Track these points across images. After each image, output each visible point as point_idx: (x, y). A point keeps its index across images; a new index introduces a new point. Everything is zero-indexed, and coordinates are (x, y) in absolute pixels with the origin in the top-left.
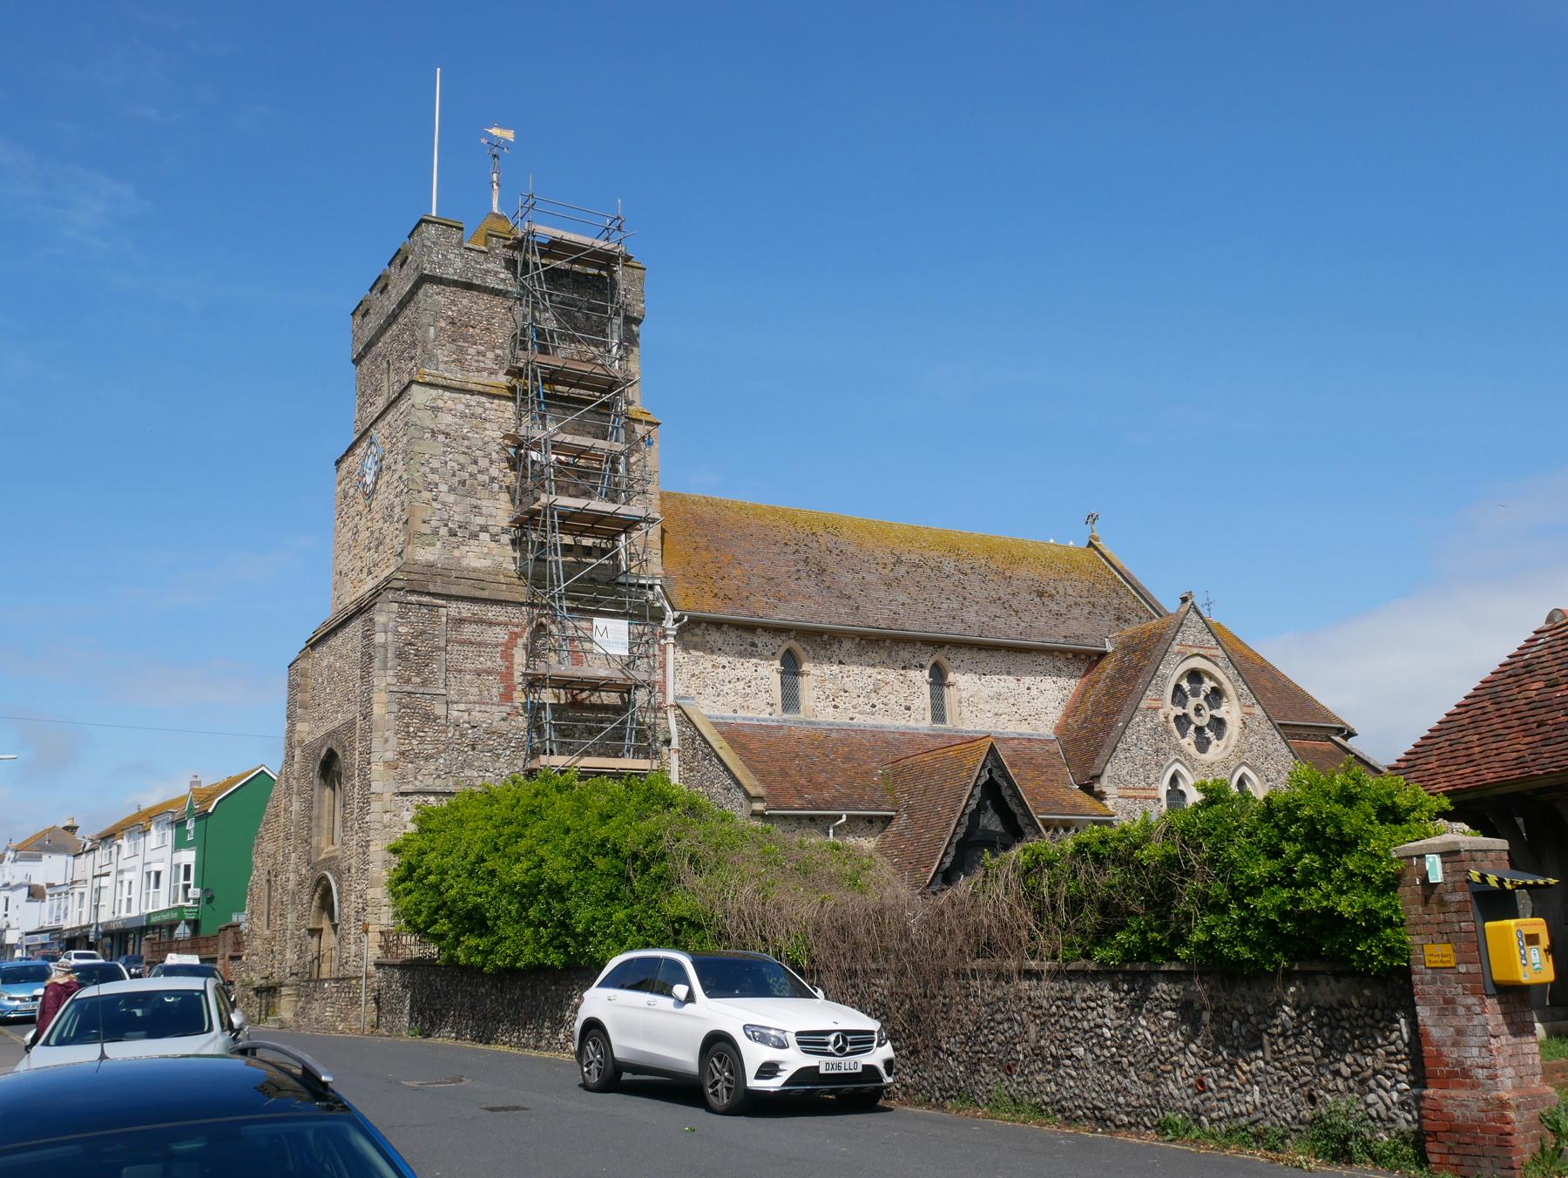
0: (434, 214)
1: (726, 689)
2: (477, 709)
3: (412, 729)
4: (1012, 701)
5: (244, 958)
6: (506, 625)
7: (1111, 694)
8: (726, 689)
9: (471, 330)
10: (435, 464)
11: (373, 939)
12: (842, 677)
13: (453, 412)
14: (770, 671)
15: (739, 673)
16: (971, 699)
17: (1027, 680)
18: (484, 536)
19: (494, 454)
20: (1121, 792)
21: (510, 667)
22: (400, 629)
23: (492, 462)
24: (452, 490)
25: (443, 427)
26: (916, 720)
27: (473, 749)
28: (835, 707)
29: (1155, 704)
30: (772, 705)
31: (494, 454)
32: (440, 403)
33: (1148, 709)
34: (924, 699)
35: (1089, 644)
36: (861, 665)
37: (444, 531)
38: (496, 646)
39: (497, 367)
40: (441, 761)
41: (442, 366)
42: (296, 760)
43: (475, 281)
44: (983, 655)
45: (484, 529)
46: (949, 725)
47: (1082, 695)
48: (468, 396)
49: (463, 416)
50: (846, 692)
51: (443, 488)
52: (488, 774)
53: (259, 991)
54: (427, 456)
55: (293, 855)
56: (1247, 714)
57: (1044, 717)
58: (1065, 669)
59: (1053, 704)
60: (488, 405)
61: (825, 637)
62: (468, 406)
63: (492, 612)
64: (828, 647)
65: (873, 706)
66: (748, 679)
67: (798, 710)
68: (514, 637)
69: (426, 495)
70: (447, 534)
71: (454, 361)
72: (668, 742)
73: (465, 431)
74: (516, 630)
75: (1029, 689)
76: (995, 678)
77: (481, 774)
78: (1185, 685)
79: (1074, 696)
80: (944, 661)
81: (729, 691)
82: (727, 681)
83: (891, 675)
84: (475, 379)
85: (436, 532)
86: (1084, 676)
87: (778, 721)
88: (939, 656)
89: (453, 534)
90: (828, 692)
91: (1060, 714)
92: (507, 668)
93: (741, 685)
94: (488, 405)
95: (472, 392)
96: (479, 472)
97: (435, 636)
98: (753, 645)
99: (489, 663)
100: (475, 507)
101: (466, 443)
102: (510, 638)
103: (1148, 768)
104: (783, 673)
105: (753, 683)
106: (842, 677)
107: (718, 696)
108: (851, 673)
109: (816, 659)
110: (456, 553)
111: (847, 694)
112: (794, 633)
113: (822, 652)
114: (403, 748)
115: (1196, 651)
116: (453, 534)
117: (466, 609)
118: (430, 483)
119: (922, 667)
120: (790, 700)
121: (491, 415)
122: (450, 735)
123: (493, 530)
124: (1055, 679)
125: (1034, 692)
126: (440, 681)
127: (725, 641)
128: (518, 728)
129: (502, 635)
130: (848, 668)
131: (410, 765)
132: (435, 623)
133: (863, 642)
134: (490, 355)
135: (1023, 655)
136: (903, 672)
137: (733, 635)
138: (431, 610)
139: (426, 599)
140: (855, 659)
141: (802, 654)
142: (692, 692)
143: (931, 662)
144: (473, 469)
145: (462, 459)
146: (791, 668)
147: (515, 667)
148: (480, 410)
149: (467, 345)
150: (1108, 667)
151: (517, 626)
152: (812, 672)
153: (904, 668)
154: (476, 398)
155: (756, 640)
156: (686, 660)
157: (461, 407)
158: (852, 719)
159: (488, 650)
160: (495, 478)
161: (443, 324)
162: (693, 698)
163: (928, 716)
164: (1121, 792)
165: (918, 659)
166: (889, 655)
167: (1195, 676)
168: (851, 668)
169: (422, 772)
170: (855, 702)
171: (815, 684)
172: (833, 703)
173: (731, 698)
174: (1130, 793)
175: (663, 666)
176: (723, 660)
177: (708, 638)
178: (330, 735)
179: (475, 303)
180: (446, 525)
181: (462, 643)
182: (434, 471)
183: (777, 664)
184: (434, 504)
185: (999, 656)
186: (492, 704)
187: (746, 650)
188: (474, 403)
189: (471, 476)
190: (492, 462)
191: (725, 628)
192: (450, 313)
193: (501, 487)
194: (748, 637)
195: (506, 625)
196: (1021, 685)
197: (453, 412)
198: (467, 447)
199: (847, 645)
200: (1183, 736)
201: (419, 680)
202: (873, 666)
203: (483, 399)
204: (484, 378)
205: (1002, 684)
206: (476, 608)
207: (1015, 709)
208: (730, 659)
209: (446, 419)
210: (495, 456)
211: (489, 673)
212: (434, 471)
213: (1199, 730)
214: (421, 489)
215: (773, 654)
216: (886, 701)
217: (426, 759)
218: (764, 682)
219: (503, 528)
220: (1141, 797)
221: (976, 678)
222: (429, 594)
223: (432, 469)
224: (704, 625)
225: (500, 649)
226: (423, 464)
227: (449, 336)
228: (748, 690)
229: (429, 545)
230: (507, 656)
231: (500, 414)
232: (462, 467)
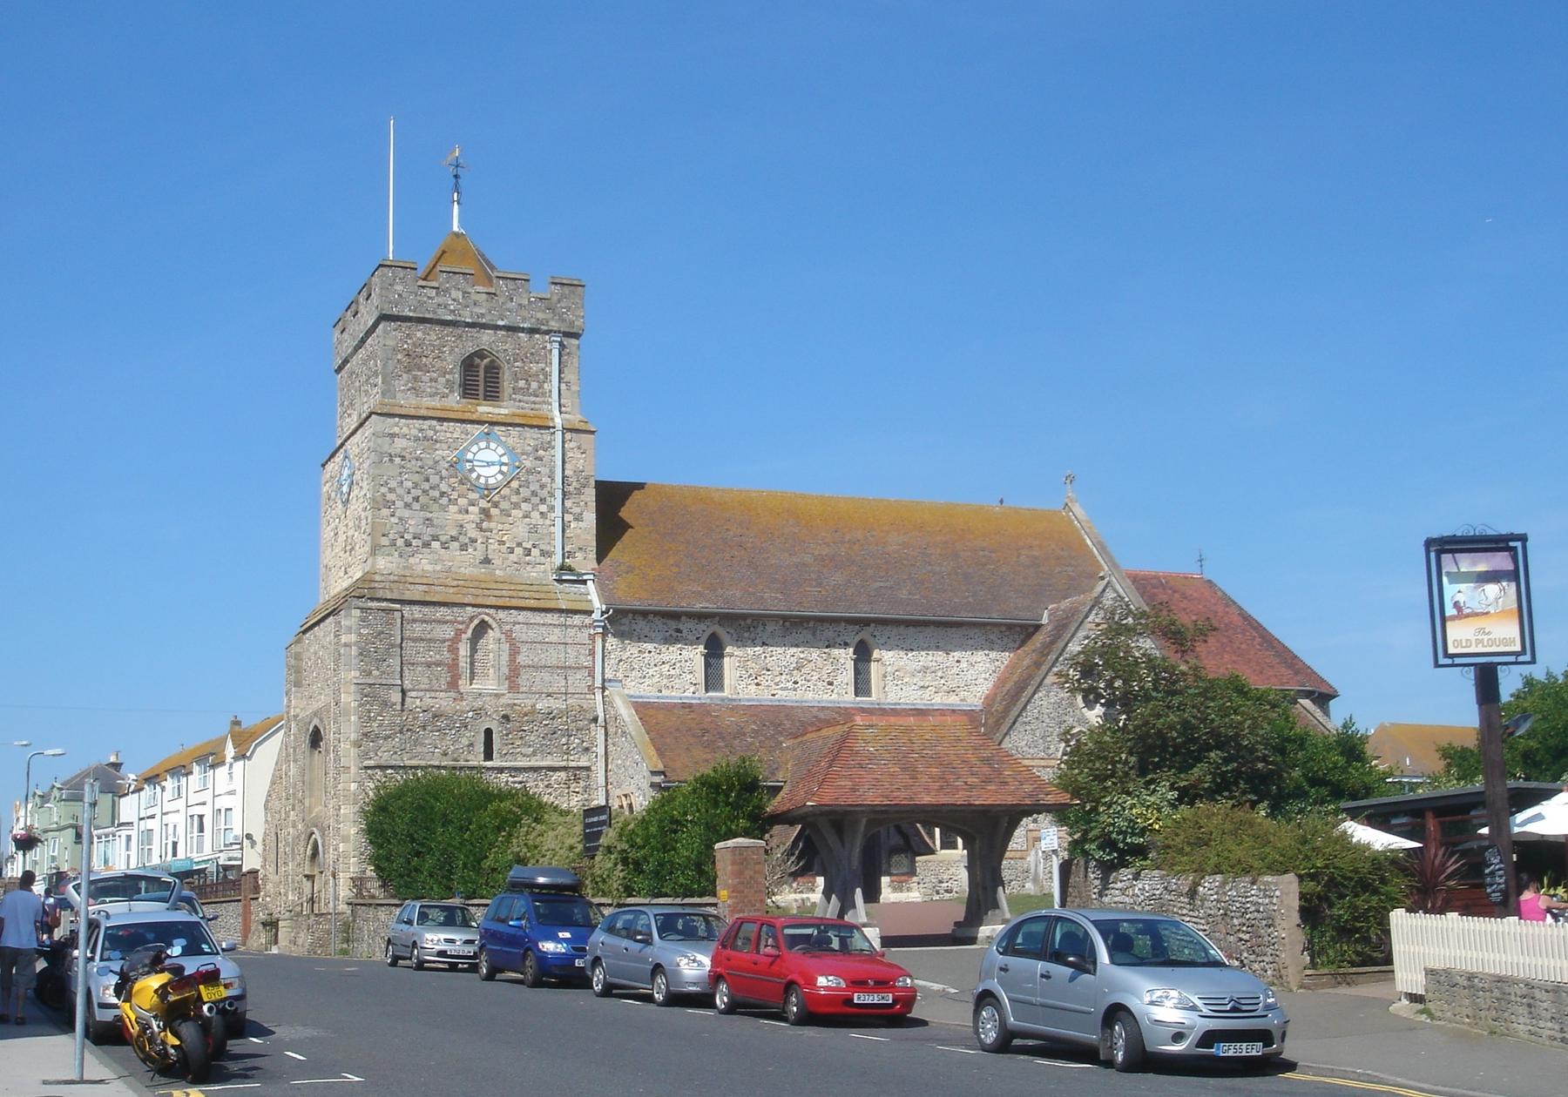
0: (391, 258)
1: (651, 672)
2: (428, 696)
3: (372, 715)
4: (940, 674)
5: (260, 899)
6: (452, 622)
7: (1038, 665)
8: (651, 672)
9: (424, 359)
10: (393, 484)
11: (344, 879)
13: (408, 437)
14: (695, 656)
15: (665, 657)
16: (897, 673)
17: (957, 655)
18: (436, 545)
19: (444, 471)
21: (456, 659)
22: (362, 631)
23: (442, 478)
24: (407, 506)
25: (398, 451)
26: (838, 694)
27: (425, 730)
28: (757, 684)
30: (695, 684)
31: (444, 471)
32: (396, 430)
34: (847, 676)
35: (1024, 616)
36: (785, 645)
37: (400, 542)
38: (444, 641)
39: (447, 391)
40: (397, 740)
41: (399, 395)
42: (292, 732)
43: (427, 316)
44: (911, 629)
45: (435, 538)
46: (874, 698)
47: (1012, 667)
48: (421, 422)
49: (417, 439)
50: (769, 670)
51: (399, 504)
52: (437, 750)
53: (264, 924)
54: (385, 478)
55: (292, 812)
57: (973, 688)
58: (999, 641)
59: (983, 676)
60: (438, 428)
62: (421, 430)
63: (442, 612)
64: (752, 629)
65: (796, 683)
66: (673, 661)
67: (721, 689)
68: (459, 633)
69: (385, 512)
70: (403, 545)
71: (408, 390)
72: (595, 720)
73: (418, 452)
74: (460, 627)
75: (958, 661)
76: (923, 653)
77: (431, 750)
79: (1006, 667)
80: (870, 641)
81: (655, 674)
82: (652, 664)
83: (815, 654)
84: (428, 403)
85: (393, 543)
86: (1018, 648)
87: (700, 699)
88: (865, 634)
89: (408, 544)
91: (990, 685)
92: (453, 659)
93: (667, 667)
94: (438, 428)
95: (424, 418)
96: (431, 488)
97: (391, 636)
98: (679, 631)
99: (438, 656)
100: (428, 520)
101: (419, 463)
102: (456, 634)
103: (1049, 739)
104: (706, 656)
105: (678, 665)
106: (765, 657)
107: (645, 677)
108: (774, 653)
109: (741, 642)
110: (411, 560)
111: (770, 673)
112: (717, 618)
113: (746, 635)
114: (365, 730)
116: (408, 544)
117: (417, 612)
118: (388, 501)
119: (846, 645)
120: (713, 678)
121: (441, 435)
122: (404, 718)
123: (443, 539)
124: (987, 652)
125: (964, 665)
126: (396, 673)
127: (651, 628)
128: (462, 712)
129: (449, 632)
130: (771, 649)
131: (371, 744)
132: (391, 624)
134: (442, 380)
135: (954, 629)
136: (826, 650)
137: (658, 622)
138: (388, 614)
139: (384, 604)
142: (620, 675)
143: (857, 639)
144: (426, 486)
145: (416, 478)
146: (714, 652)
147: (460, 658)
148: (431, 433)
149: (419, 373)
150: (1039, 639)
151: (462, 623)
152: (736, 653)
153: (827, 647)
154: (428, 422)
155: (681, 627)
156: (614, 647)
157: (414, 432)
158: (773, 695)
159: (436, 645)
160: (445, 493)
161: (399, 357)
162: (621, 681)
163: (852, 689)
166: (814, 634)
169: (382, 749)
170: (777, 679)
171: (737, 664)
172: (756, 681)
173: (656, 679)
175: (592, 653)
176: (649, 646)
177: (634, 626)
178: (315, 714)
179: (428, 334)
180: (403, 537)
181: (415, 640)
182: (391, 490)
183: (701, 648)
184: (392, 519)
185: (929, 631)
186: (441, 691)
187: (671, 635)
188: (425, 427)
189: (423, 492)
190: (442, 478)
191: (651, 617)
192: (406, 346)
193: (450, 500)
194: (673, 624)
195: (452, 622)
196: (951, 659)
197: (408, 437)
198: (422, 467)
199: (770, 627)
200: (1091, 708)
201: (378, 673)
203: (434, 423)
204: (436, 402)
205: (930, 658)
206: (426, 610)
207: (942, 681)
208: (656, 645)
209: (400, 443)
210: (444, 473)
211: (438, 665)
212: (391, 490)
214: (381, 507)
216: (808, 677)
217: (386, 738)
218: (688, 664)
219: (452, 537)
221: (902, 653)
222: (386, 600)
223: (389, 489)
224: (630, 615)
225: (447, 644)
226: (382, 485)
227: (405, 367)
228: (672, 672)
229: (388, 555)
230: (454, 650)
231: (449, 435)
232: (416, 485)
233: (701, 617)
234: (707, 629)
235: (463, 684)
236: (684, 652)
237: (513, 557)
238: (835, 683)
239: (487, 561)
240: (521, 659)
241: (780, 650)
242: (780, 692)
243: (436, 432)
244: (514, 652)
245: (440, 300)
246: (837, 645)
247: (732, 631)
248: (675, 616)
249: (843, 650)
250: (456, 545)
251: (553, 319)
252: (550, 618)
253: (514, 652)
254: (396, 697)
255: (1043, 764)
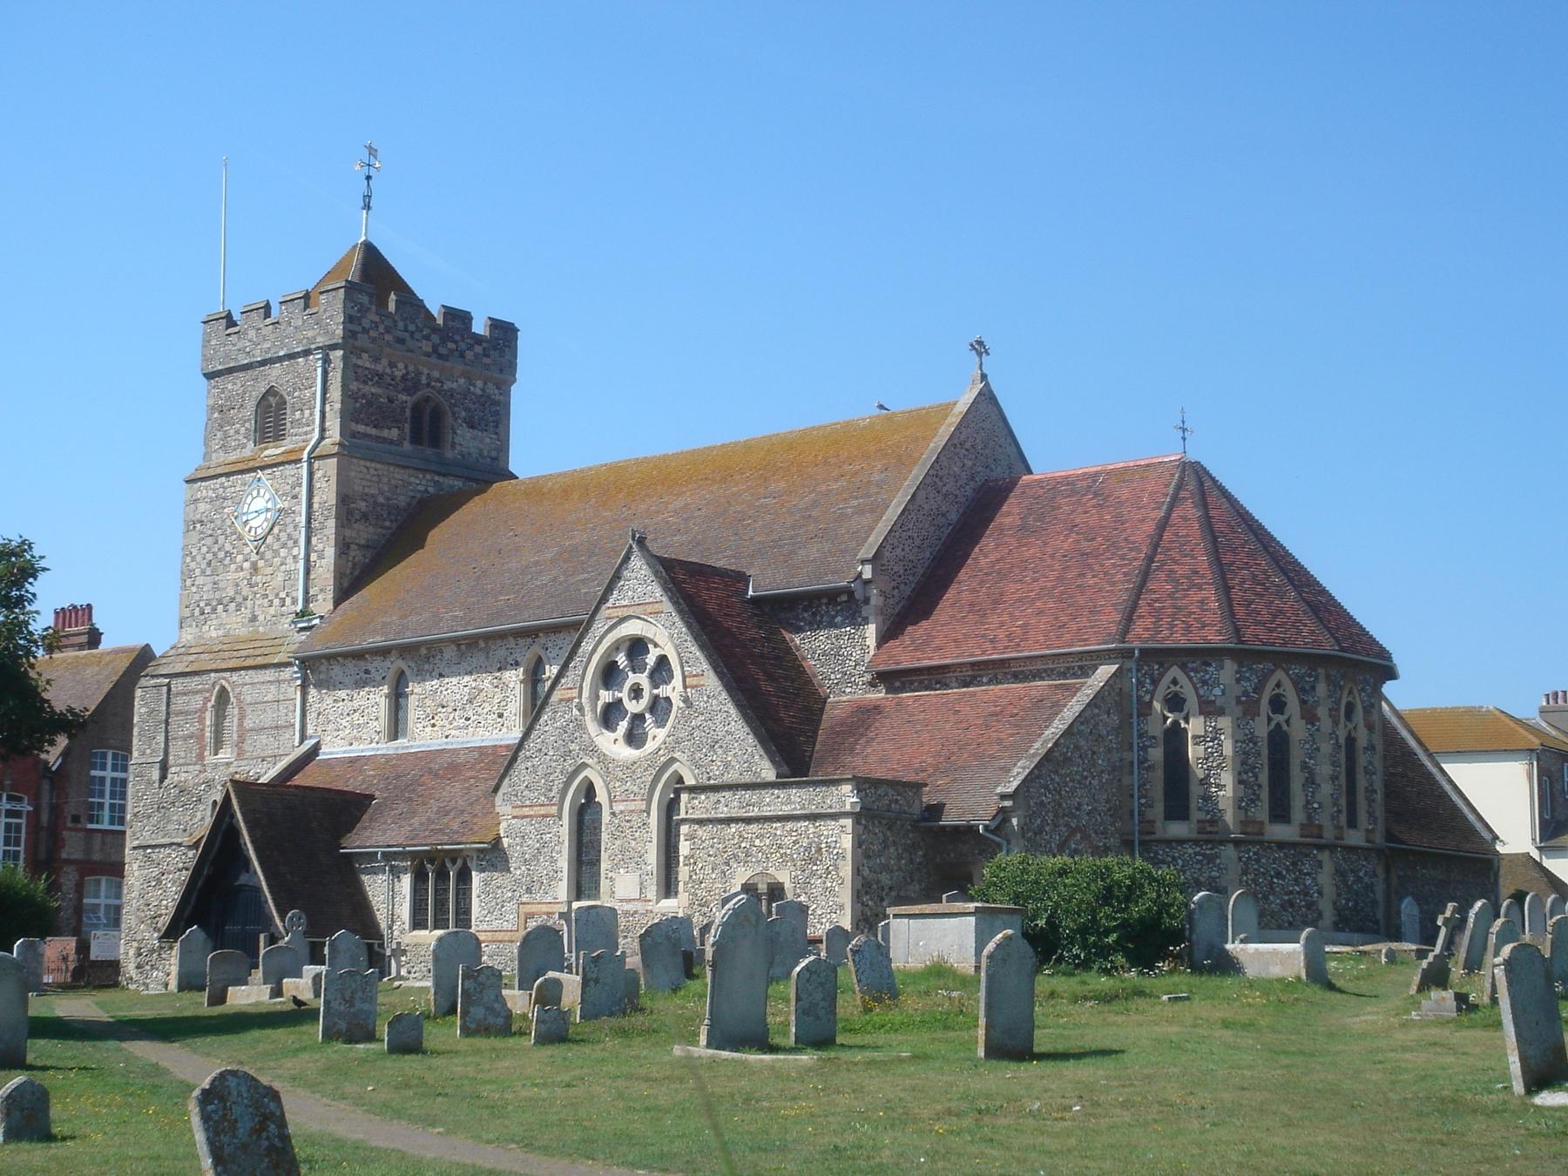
12: (441, 692)
14: (376, 699)
20: (518, 812)
29: (569, 694)
33: (561, 700)
50: (443, 707)
56: (693, 687)
61: (423, 651)
68: (207, 700)
78: (622, 660)
83: (486, 681)
90: (428, 710)
98: (367, 672)
105: (366, 711)
109: (422, 675)
111: (444, 710)
115: (630, 612)
119: (517, 664)
120: (396, 728)
130: (447, 680)
133: (463, 647)
137: (350, 664)
140: (454, 668)
141: (408, 673)
143: (529, 654)
153: (500, 669)
158: (447, 737)
164: (518, 812)
165: (513, 656)
167: (637, 647)
168: (451, 679)
172: (432, 721)
174: (526, 811)
176: (342, 694)
202: (471, 673)
208: (349, 692)
211: (191, 737)
213: (638, 718)
215: (383, 678)
220: (537, 816)
230: (201, 720)
233: (384, 652)
234: (396, 664)
235: (210, 759)
236: (371, 696)
237: (272, 611)
238: (505, 715)
239: (254, 619)
240: (248, 724)
241: (454, 680)
242: (453, 732)
243: (225, 488)
244: (242, 718)
245: (240, 345)
246: (509, 666)
247: (413, 665)
248: (359, 655)
249: (514, 671)
250: (233, 605)
251: (319, 334)
252: (269, 675)
253: (242, 718)
254: (156, 775)
255: (542, 812)
